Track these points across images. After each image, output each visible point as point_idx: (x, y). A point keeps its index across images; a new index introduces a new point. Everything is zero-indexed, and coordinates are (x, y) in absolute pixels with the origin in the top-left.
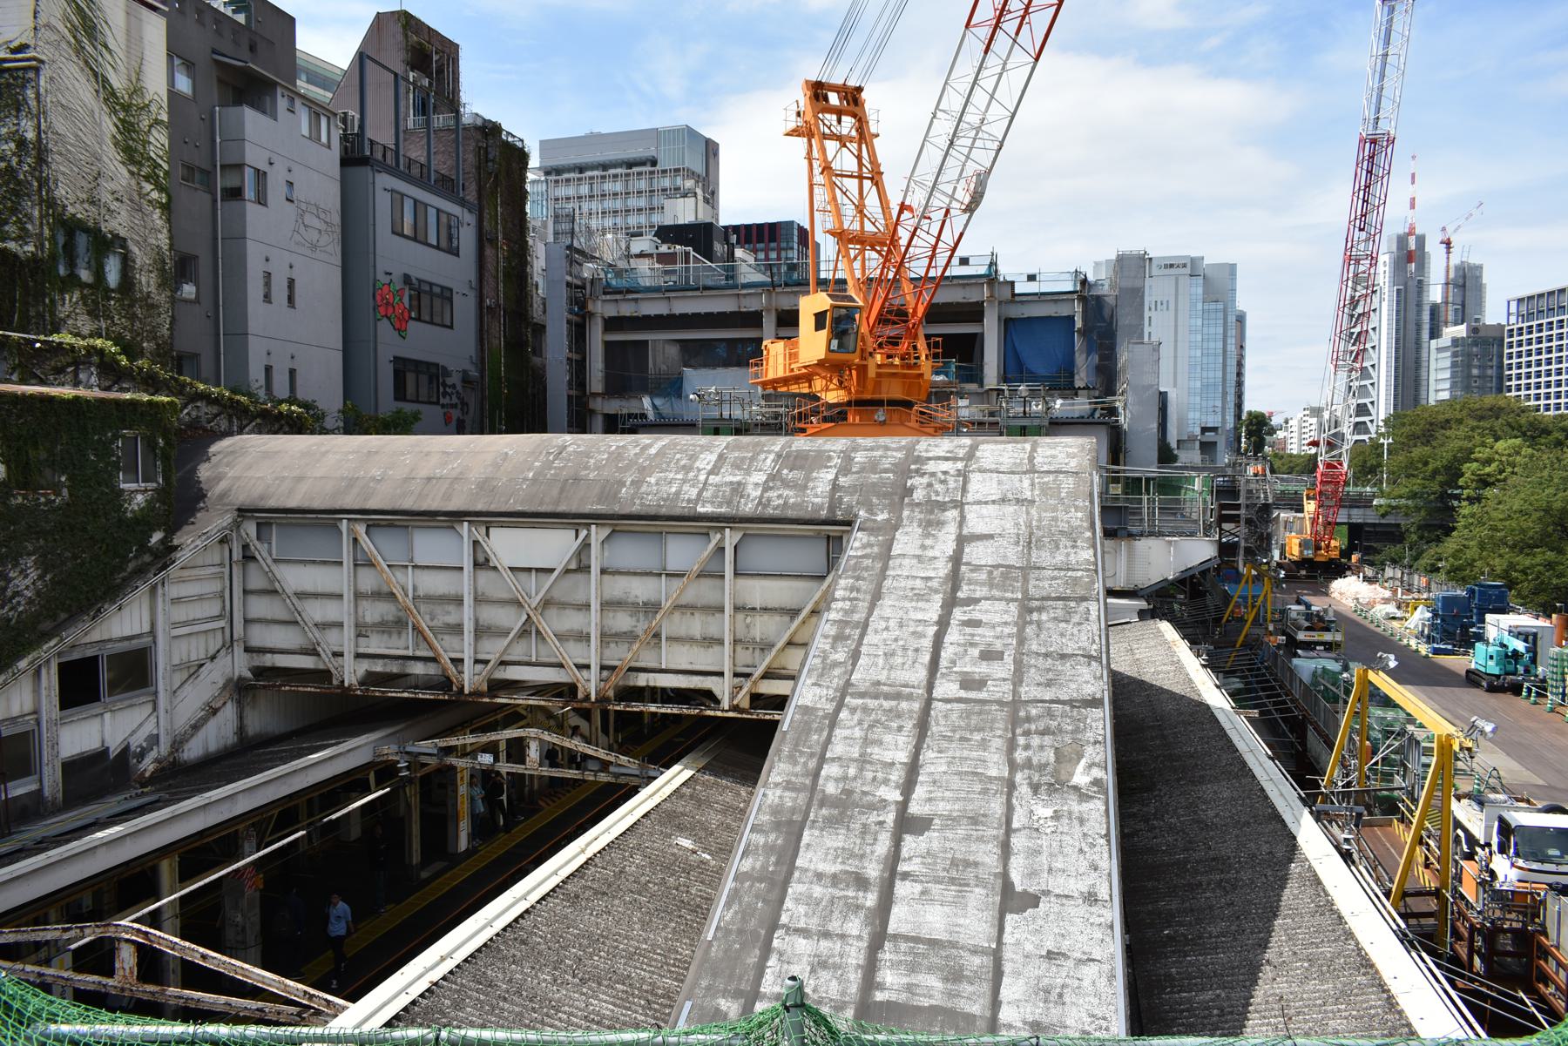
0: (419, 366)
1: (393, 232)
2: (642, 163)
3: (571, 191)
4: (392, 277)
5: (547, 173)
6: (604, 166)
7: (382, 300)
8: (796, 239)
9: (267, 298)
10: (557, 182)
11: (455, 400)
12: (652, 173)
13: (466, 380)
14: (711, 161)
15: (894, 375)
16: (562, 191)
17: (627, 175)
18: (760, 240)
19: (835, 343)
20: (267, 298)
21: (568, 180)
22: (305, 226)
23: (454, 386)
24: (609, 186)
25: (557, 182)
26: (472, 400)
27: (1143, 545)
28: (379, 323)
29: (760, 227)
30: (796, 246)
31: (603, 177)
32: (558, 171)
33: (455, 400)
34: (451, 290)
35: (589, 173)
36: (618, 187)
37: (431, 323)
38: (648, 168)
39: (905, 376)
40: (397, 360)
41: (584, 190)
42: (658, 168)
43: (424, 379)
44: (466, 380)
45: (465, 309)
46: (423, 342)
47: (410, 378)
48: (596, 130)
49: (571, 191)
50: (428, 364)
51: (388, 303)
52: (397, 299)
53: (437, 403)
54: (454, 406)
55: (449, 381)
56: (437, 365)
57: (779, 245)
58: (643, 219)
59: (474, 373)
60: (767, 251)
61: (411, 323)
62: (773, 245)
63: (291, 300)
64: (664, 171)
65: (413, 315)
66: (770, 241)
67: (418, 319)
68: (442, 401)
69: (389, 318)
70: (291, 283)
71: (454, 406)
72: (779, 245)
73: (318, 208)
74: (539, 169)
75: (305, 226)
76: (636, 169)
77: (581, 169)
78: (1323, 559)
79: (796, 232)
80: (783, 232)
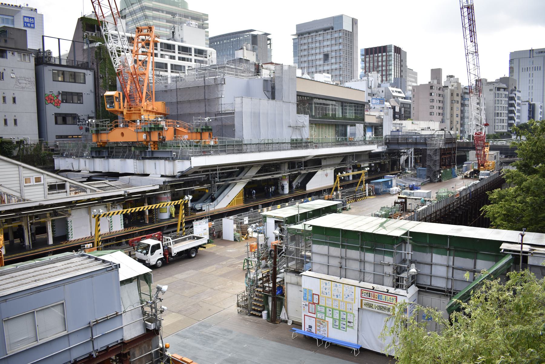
2: (329, 29)
5: (299, 36)
6: (317, 31)
7: (49, 98)
8: (393, 51)
10: (301, 38)
12: (331, 32)
14: (354, 26)
16: (303, 41)
17: (324, 34)
18: (371, 54)
19: (108, 106)
21: (305, 37)
24: (318, 38)
25: (301, 38)
27: (177, 161)
29: (380, 48)
30: (393, 53)
31: (316, 35)
36: (321, 38)
38: (331, 31)
41: (310, 40)
42: (334, 30)
48: (315, 19)
52: (55, 98)
57: (386, 54)
58: (329, 49)
62: (384, 54)
64: (336, 31)
66: (384, 52)
72: (378, 55)
74: (296, 34)
76: (327, 31)
77: (309, 33)
79: (393, 49)
80: (388, 49)
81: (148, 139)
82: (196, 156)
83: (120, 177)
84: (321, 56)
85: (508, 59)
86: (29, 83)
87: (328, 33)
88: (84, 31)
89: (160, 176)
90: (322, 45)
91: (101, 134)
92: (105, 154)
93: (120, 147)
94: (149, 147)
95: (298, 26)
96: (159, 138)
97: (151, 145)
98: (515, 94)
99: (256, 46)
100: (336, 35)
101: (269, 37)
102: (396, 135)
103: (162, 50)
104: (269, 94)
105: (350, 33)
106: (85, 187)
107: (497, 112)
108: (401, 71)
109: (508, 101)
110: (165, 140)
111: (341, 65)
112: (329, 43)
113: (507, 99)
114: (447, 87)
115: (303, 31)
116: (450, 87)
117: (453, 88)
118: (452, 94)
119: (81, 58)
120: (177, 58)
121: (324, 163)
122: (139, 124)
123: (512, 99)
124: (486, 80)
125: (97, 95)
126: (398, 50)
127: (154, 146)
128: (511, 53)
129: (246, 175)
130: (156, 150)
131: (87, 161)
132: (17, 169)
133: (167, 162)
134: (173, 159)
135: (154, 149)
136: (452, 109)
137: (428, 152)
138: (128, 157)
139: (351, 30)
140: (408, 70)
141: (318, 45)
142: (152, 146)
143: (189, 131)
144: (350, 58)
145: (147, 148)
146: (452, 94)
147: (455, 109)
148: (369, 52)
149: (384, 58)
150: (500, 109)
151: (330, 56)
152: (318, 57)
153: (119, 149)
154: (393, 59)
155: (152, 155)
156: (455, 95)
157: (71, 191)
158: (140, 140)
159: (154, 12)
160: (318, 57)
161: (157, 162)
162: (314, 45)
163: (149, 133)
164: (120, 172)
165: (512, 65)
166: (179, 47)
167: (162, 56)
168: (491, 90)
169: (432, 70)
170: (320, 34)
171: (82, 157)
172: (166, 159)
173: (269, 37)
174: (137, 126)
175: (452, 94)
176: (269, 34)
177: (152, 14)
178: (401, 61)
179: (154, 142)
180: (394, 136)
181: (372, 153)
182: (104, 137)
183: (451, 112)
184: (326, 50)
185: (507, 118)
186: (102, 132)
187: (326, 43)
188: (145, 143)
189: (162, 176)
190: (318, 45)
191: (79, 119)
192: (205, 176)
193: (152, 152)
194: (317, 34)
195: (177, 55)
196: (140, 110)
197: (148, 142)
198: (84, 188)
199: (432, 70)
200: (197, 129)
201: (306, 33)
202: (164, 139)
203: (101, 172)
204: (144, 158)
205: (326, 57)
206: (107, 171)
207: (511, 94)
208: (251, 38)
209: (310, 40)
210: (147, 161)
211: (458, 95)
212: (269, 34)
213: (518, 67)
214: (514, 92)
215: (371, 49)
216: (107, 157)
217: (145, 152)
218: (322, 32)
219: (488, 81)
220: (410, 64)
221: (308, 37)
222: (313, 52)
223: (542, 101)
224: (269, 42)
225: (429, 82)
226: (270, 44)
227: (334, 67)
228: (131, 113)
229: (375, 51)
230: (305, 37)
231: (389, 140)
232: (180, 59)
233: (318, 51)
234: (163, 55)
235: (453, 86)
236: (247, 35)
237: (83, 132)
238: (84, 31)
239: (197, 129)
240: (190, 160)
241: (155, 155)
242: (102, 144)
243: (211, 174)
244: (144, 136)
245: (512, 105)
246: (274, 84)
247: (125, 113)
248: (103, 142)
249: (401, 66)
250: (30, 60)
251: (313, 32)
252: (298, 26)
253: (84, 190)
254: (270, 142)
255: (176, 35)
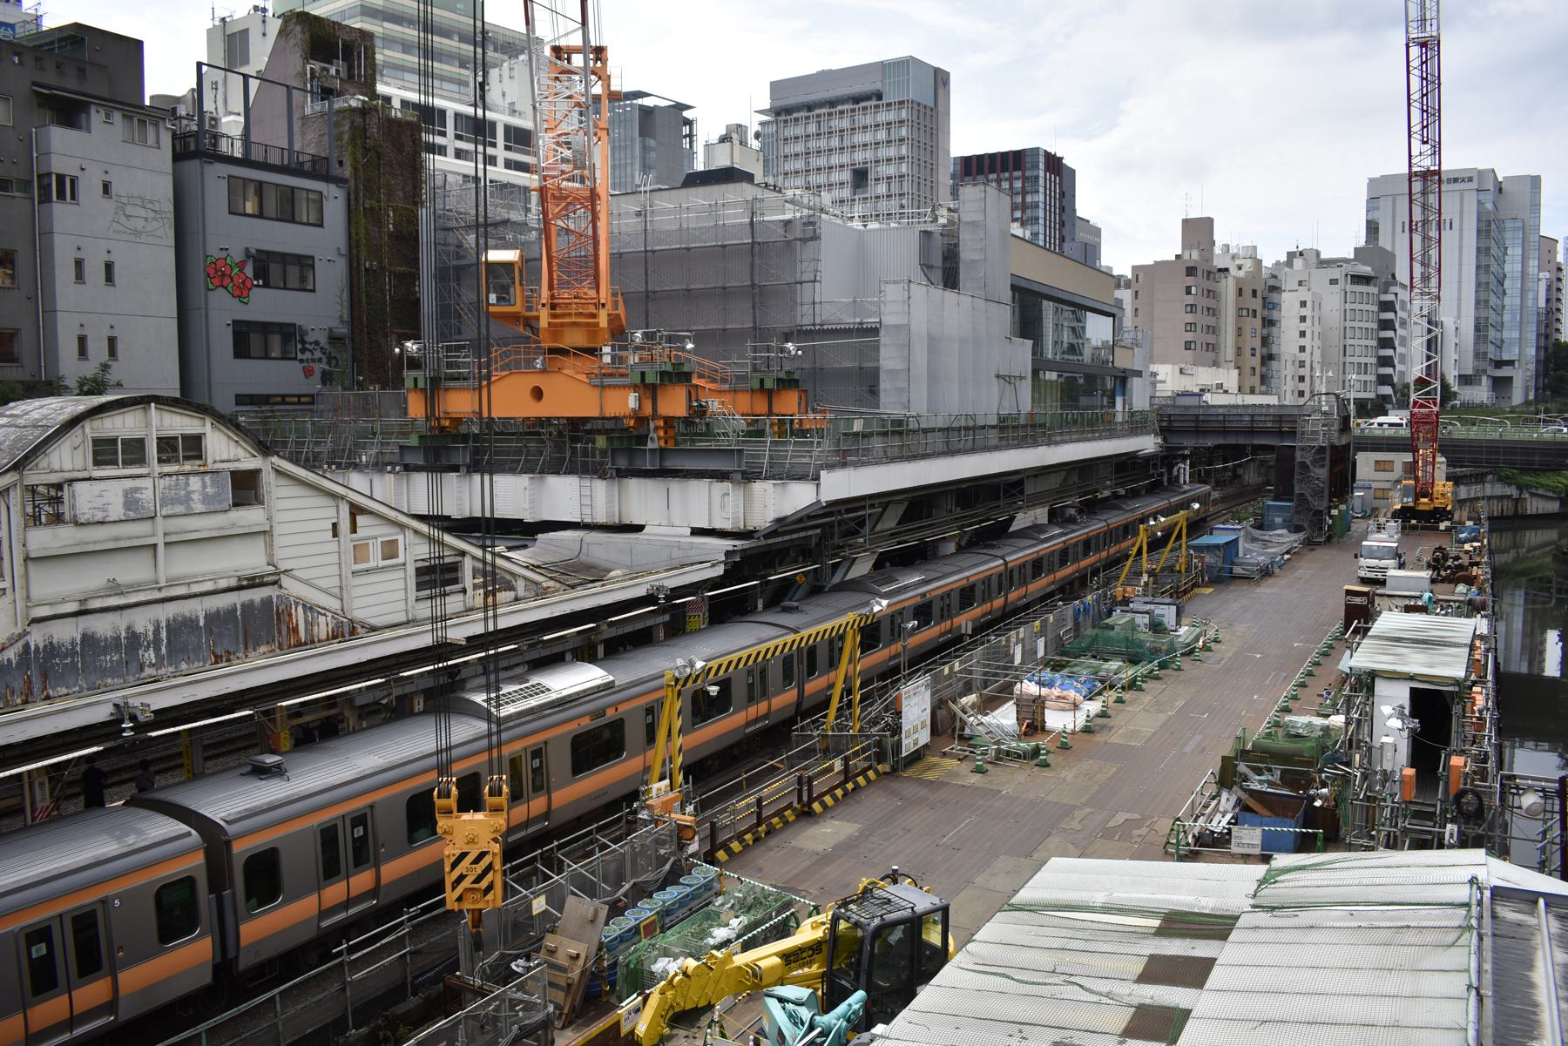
0: (266, 328)
1: (230, 213)
2: (867, 98)
3: (799, 131)
4: (231, 252)
6: (832, 103)
9: (80, 277)
10: (786, 121)
11: (318, 354)
13: (334, 339)
14: (941, 91)
15: (574, 324)
16: (792, 131)
17: (853, 111)
19: (493, 298)
20: (80, 277)
21: (796, 120)
22: (128, 217)
23: (317, 343)
24: (836, 123)
25: (786, 121)
26: (344, 357)
27: (759, 487)
28: (210, 293)
29: (1004, 155)
30: (1042, 174)
31: (830, 114)
32: (788, 110)
33: (318, 354)
34: (313, 258)
35: (840, 108)
37: (285, 288)
38: (874, 102)
39: (588, 325)
40: (234, 321)
41: (812, 128)
43: (276, 341)
44: (334, 339)
45: (331, 276)
46: (268, 305)
47: (255, 340)
49: (799, 131)
50: (281, 325)
51: (224, 275)
53: (295, 359)
54: (320, 360)
55: (308, 339)
56: (294, 325)
57: (1023, 174)
59: (344, 330)
60: (1011, 180)
61: (255, 292)
63: (109, 278)
65: (261, 282)
67: (266, 285)
68: (300, 356)
69: (226, 288)
70: (109, 267)
71: (320, 360)
73: (143, 199)
75: (128, 217)
77: (810, 107)
78: (1426, 508)
81: (648, 410)
82: (830, 467)
83: (540, 536)
84: (846, 176)
85: (1364, 197)
86: (154, 219)
87: (865, 109)
88: (306, 60)
89: (689, 531)
90: (847, 143)
91: (447, 390)
92: (463, 458)
93: (513, 434)
94: (652, 435)
95: (777, 87)
96: (690, 407)
97: (657, 428)
98: (1396, 294)
99: (652, 143)
100: (892, 116)
101: (686, 114)
102: (1191, 407)
103: (458, 137)
104: (937, 275)
105: (928, 111)
106: (512, 574)
107: (1349, 342)
108: (1062, 224)
109: (1378, 313)
110: (704, 413)
111: (904, 202)
112: (868, 137)
113: (1375, 308)
114: (1227, 270)
115: (792, 101)
116: (1233, 271)
117: (1241, 274)
118: (1240, 292)
119: (309, 144)
120: (500, 162)
121: (1029, 489)
122: (607, 359)
123: (1387, 306)
124: (1318, 253)
125: (355, 264)
126: (1054, 164)
127: (666, 433)
128: (1371, 180)
129: (878, 528)
130: (671, 445)
131: (377, 479)
132: (332, 512)
133: (727, 485)
134: (749, 476)
135: (666, 442)
136: (1239, 332)
137: (1298, 455)
138: (556, 468)
139: (931, 104)
140: (1078, 222)
141: (835, 142)
142: (661, 433)
143: (726, 387)
144: (928, 183)
145: (643, 439)
146: (1240, 289)
147: (1247, 332)
148: (976, 167)
149: (1018, 184)
150: (1358, 334)
151: (871, 176)
152: (836, 177)
153: (511, 441)
154: (1041, 190)
155: (630, 463)
156: (1247, 293)
157: (475, 587)
158: (610, 411)
159: (386, 25)
160: (836, 177)
161: (675, 485)
162: (823, 144)
163: (649, 390)
164: (528, 518)
165: (1375, 215)
166: (507, 128)
167: (459, 154)
168: (1333, 282)
169: (1186, 222)
170: (842, 112)
171: (356, 467)
172: (721, 476)
173: (686, 114)
174: (601, 368)
175: (1240, 289)
176: (689, 107)
177: (380, 30)
178: (1063, 194)
179: (669, 421)
180: (1186, 407)
181: (1137, 457)
182: (459, 403)
183: (1237, 342)
184: (859, 156)
185: (1374, 360)
186: (452, 384)
187: (859, 138)
188: (632, 423)
189: (696, 532)
190: (835, 142)
191: (303, 342)
192: (818, 531)
193: (662, 450)
194: (833, 110)
195: (500, 152)
196: (594, 316)
197: (641, 420)
198: (508, 577)
199: (1186, 222)
200: (762, 381)
201: (798, 108)
202: (701, 411)
203: (448, 518)
204: (622, 474)
205: (860, 177)
206: (467, 514)
207: (1386, 292)
208: (637, 113)
209: (812, 128)
210: (633, 484)
211: (1254, 293)
212: (689, 107)
213: (1390, 220)
214: (1393, 289)
215: (980, 158)
216: (468, 467)
217: (631, 453)
218: (845, 107)
219: (1323, 256)
220: (1085, 205)
221: (807, 118)
222: (822, 162)
223: (1455, 314)
224: (686, 130)
225: (1178, 257)
226: (690, 136)
227: (883, 206)
228: (562, 325)
229: (990, 166)
230: (796, 120)
231: (1170, 421)
232: (509, 164)
233: (836, 160)
234: (462, 150)
235: (1240, 268)
236: (626, 106)
237: (315, 385)
238: (306, 60)
239: (762, 381)
240: (817, 478)
241: (672, 463)
242: (447, 423)
243: (840, 523)
244: (632, 401)
245: (1387, 325)
246: (956, 245)
247: (544, 322)
248: (451, 419)
249: (1062, 209)
250: (158, 142)
251: (821, 104)
252: (777, 87)
253: (509, 582)
254: (971, 424)
255: (493, 95)
